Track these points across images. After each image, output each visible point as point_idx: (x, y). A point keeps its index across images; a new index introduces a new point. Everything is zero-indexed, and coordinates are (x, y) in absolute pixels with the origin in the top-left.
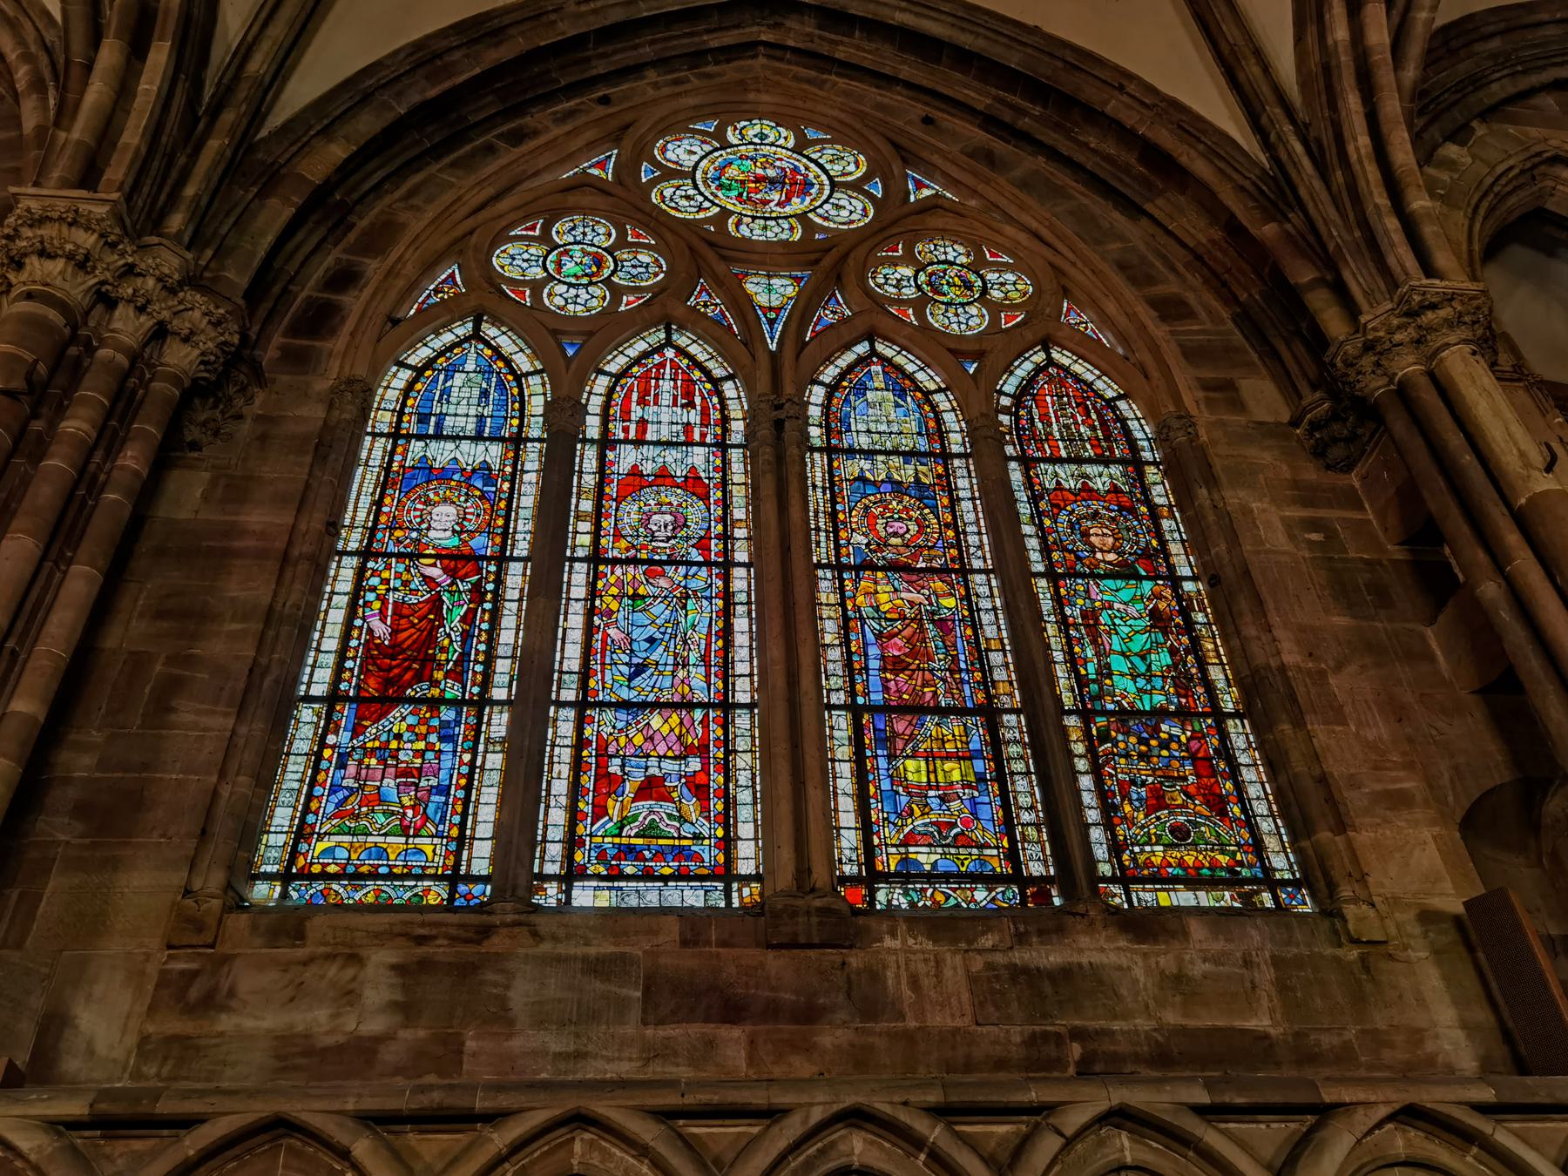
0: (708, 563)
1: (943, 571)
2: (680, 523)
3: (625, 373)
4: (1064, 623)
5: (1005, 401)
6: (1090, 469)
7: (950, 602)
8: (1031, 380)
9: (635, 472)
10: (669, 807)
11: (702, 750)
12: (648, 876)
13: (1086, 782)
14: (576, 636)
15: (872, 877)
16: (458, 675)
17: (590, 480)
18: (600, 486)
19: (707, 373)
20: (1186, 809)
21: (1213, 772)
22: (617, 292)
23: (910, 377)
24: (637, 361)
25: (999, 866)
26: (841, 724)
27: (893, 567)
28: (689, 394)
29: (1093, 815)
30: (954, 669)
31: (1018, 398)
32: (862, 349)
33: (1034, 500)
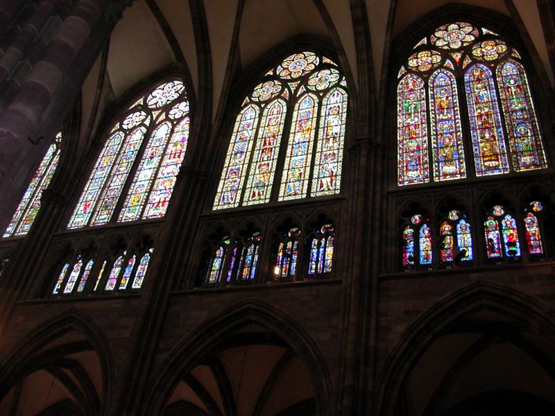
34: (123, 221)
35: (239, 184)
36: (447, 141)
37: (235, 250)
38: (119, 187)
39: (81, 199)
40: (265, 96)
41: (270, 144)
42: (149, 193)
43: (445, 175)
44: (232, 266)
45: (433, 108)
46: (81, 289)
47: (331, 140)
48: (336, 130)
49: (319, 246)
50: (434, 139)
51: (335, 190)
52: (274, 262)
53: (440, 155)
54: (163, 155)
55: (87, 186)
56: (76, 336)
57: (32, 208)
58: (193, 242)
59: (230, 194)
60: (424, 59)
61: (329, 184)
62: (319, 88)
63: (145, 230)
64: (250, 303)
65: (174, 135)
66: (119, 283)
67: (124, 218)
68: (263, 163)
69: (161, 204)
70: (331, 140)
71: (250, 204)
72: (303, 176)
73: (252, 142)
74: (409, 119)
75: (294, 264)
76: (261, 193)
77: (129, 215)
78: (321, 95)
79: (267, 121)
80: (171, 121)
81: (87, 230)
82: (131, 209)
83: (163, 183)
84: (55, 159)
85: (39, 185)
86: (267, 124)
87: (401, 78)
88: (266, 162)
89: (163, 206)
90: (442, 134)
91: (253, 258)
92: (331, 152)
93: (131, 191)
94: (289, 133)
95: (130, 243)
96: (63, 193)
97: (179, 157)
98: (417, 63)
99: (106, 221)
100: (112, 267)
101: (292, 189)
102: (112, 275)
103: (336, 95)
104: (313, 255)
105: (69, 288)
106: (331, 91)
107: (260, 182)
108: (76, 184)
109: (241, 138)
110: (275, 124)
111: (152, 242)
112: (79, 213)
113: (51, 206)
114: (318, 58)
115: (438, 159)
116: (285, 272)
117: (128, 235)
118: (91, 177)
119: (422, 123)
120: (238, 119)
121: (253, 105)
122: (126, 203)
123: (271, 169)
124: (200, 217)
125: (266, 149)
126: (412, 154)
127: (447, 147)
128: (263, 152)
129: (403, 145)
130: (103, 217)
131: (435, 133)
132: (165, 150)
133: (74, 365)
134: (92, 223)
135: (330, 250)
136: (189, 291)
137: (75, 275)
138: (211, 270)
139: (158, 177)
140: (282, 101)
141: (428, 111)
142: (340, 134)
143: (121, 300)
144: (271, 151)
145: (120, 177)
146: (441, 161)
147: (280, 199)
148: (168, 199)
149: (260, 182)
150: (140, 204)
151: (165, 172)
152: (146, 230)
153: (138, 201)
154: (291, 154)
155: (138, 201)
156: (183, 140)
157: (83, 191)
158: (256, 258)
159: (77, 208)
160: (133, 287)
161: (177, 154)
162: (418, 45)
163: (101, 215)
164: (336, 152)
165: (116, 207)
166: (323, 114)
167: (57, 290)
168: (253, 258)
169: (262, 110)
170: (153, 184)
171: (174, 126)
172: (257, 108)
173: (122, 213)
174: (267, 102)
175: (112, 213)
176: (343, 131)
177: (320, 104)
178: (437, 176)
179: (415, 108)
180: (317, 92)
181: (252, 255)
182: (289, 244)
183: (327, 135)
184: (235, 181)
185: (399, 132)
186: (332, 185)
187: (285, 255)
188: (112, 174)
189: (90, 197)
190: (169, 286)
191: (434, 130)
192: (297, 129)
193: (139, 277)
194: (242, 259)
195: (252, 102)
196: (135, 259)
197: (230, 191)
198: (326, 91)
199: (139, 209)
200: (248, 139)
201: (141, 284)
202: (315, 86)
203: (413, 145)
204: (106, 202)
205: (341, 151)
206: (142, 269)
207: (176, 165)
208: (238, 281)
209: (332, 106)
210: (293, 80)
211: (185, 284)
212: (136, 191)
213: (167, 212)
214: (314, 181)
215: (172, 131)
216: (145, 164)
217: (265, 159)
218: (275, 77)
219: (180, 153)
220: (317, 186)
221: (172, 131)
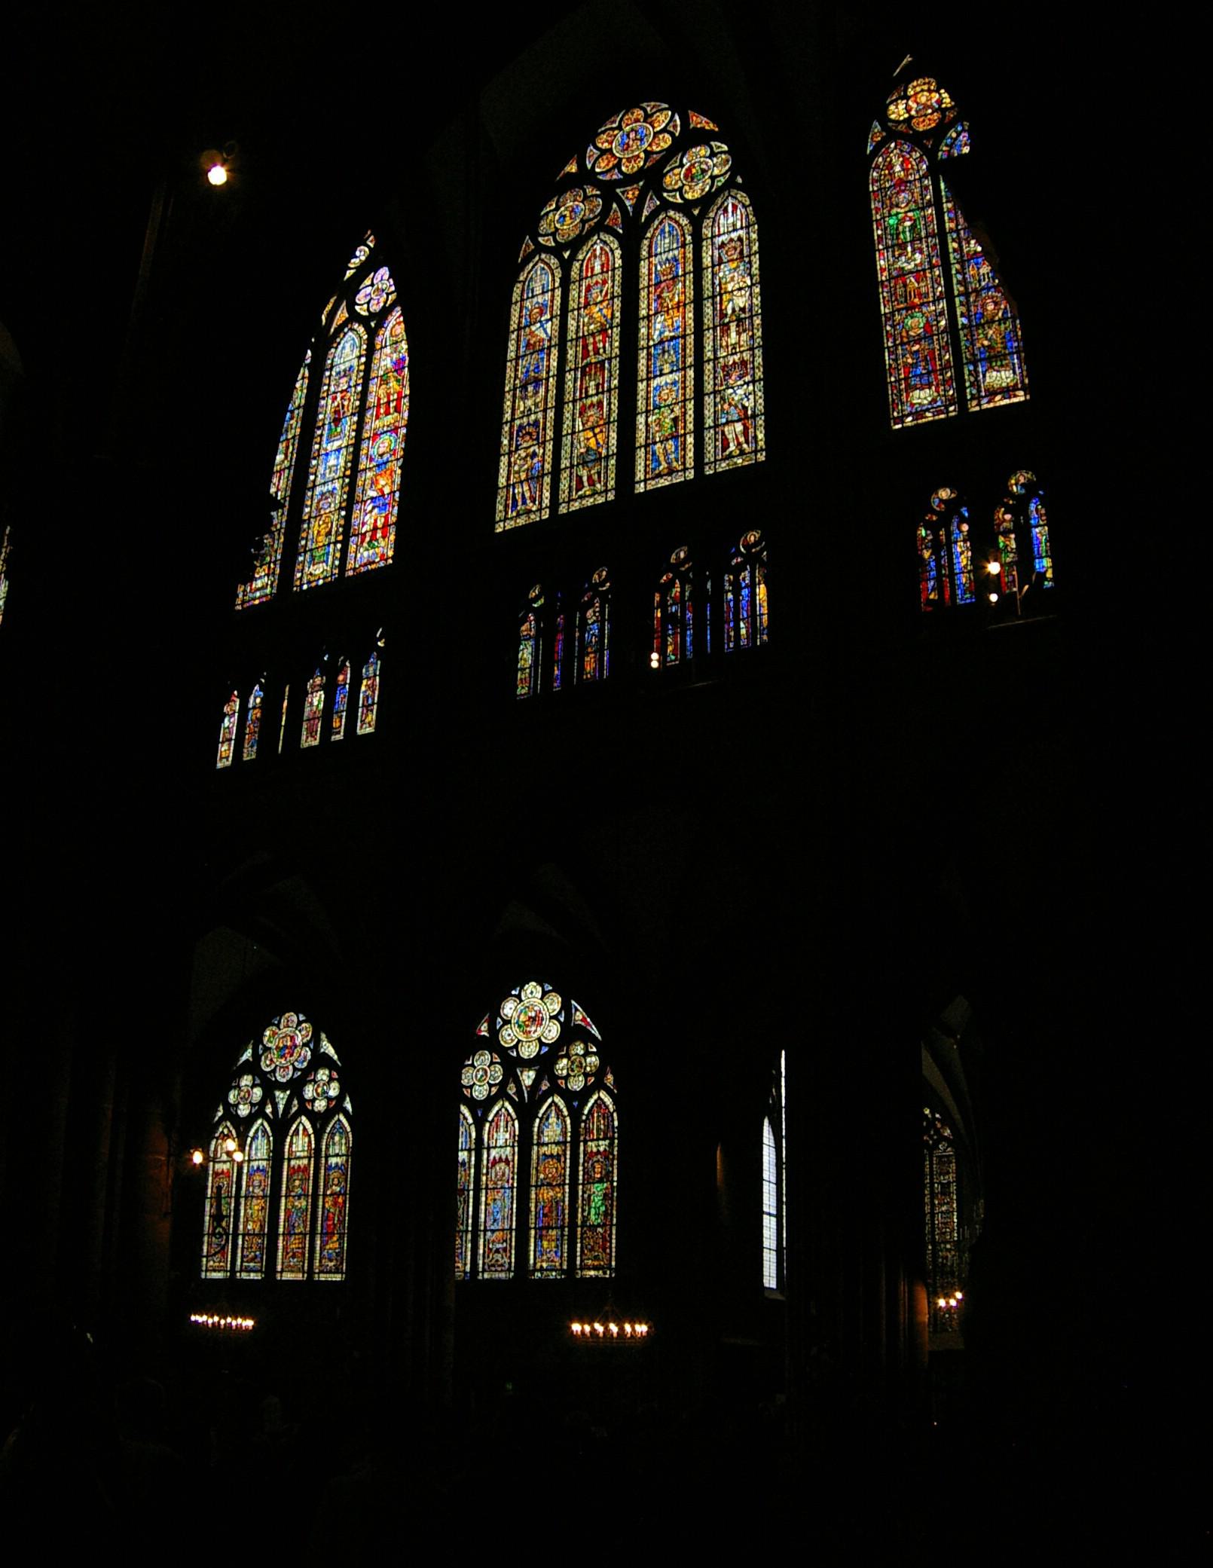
0: (509, 1188)
1: (558, 1185)
2: (504, 1174)
3: (493, 1120)
4: (583, 1200)
5: (584, 1118)
6: (601, 1143)
7: (559, 1195)
8: (592, 1107)
9: (495, 1158)
10: (500, 1255)
11: (506, 1241)
12: (496, 1271)
13: (579, 1245)
14: (483, 1211)
15: (535, 1270)
16: (462, 1224)
17: (485, 1162)
18: (488, 1162)
19: (511, 1117)
20: (599, 1253)
21: (606, 1240)
22: (491, 1086)
23: (561, 1111)
24: (496, 1115)
25: (559, 1268)
26: (533, 1232)
27: (549, 1184)
28: (507, 1127)
29: (578, 1254)
30: (557, 1215)
31: (587, 1116)
32: (550, 1100)
33: (585, 1155)
35: (544, 460)
36: (991, 307)
40: (569, 229)
41: (596, 352)
43: (992, 393)
45: (952, 225)
46: (249, 754)
47: (733, 326)
48: (741, 301)
49: (737, 589)
50: (961, 304)
51: (756, 452)
53: (978, 345)
54: (362, 411)
59: (526, 488)
60: (923, 99)
61: (742, 439)
62: (689, 196)
65: (377, 355)
66: (328, 730)
67: (305, 580)
68: (589, 401)
69: (379, 534)
70: (733, 326)
71: (576, 506)
72: (681, 424)
73: (555, 352)
74: (903, 258)
76: (596, 477)
77: (316, 571)
78: (699, 211)
79: (583, 294)
80: (364, 321)
82: (316, 554)
83: (374, 482)
86: (582, 300)
87: (875, 152)
88: (595, 399)
89: (384, 537)
90: (977, 292)
92: (736, 358)
93: (307, 510)
94: (636, 319)
97: (397, 409)
98: (908, 110)
99: (268, 590)
101: (662, 458)
103: (730, 209)
106: (720, 201)
107: (588, 449)
109: (528, 345)
110: (600, 299)
114: (677, 117)
115: (973, 354)
119: (932, 267)
120: (515, 297)
121: (543, 256)
123: (609, 416)
125: (589, 364)
126: (916, 348)
127: (991, 322)
128: (583, 374)
129: (893, 326)
130: (259, 584)
131: (962, 289)
132: (364, 395)
135: (762, 591)
139: (362, 467)
140: (609, 238)
141: (942, 234)
142: (751, 310)
144: (603, 368)
146: (981, 360)
147: (640, 488)
148: (393, 519)
149: (588, 449)
150: (333, 539)
151: (374, 452)
154: (648, 372)
155: (329, 534)
156: (398, 366)
160: (359, 732)
161: (392, 405)
162: (904, 62)
164: (746, 356)
166: (707, 261)
168: (601, 630)
169: (566, 266)
170: (352, 485)
171: (372, 334)
172: (554, 261)
174: (576, 244)
175: (278, 571)
176: (757, 301)
177: (698, 240)
178: (973, 398)
179: (913, 228)
180: (685, 208)
183: (723, 315)
184: (534, 455)
185: (884, 294)
186: (747, 442)
191: (959, 282)
192: (653, 306)
195: (541, 249)
197: (527, 480)
198: (707, 201)
200: (546, 344)
201: (373, 723)
202: (680, 190)
203: (916, 323)
205: (758, 352)
206: (369, 689)
207: (395, 430)
209: (724, 238)
210: (628, 180)
212: (318, 509)
214: (709, 435)
215: (371, 350)
216: (324, 438)
217: (592, 391)
218: (586, 177)
219: (399, 400)
220: (716, 447)
221: (371, 350)
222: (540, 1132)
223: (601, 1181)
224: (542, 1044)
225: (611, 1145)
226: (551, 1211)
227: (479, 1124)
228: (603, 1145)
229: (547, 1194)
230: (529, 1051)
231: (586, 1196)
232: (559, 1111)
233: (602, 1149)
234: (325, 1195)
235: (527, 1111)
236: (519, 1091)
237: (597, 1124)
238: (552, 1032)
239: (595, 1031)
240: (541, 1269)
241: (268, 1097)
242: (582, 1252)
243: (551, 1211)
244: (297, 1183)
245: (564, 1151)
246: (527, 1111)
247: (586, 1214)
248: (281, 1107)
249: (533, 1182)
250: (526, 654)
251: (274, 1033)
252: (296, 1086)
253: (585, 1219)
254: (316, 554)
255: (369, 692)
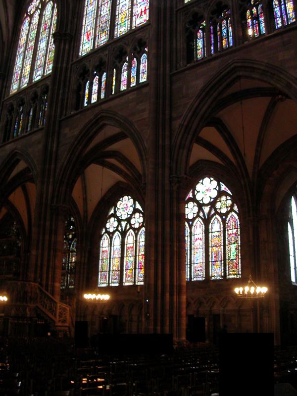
27: (216, 246)
34: (118, 36)
37: (212, 28)
38: (108, 12)
39: (83, 31)
42: (132, 8)
44: (213, 42)
46: (102, 96)
52: (245, 27)
55: (84, 21)
56: (111, 130)
57: (50, 52)
58: (176, 32)
63: (137, 36)
64: (236, 62)
67: (118, 34)
69: (143, 13)
75: (263, 25)
81: (94, 52)
82: (122, 25)
84: (54, 12)
85: (49, 34)
89: (145, 13)
91: (227, 31)
93: (117, 12)
95: (128, 49)
96: (69, 31)
100: (121, 73)
102: (123, 78)
104: (276, 14)
105: (94, 98)
108: (75, 22)
111: (145, 43)
112: (84, 42)
113: (63, 44)
116: (257, 33)
117: (125, 44)
118: (85, 14)
122: (117, 22)
124: (177, 11)
130: (102, 39)
133: (115, 154)
134: (96, 46)
136: (185, 68)
137: (95, 88)
138: (197, 50)
143: (135, 92)
145: (106, 5)
148: (147, 8)
150: (127, 19)
152: (139, 35)
153: (126, 17)
155: (126, 17)
157: (82, 26)
158: (230, 29)
159: (82, 39)
163: (101, 37)
165: (110, 28)
167: (87, 103)
168: (227, 31)
173: (116, 30)
181: (227, 29)
182: (254, 10)
187: (252, 19)
188: (100, 6)
189: (89, 28)
190: (168, 69)
193: (143, 73)
194: (219, 33)
196: (136, 61)
199: (128, 23)
201: (146, 78)
204: (102, 27)
206: (144, 66)
208: (223, 53)
211: (180, 65)
212: (121, 11)
213: (149, 18)
222: (212, 228)
223: (234, 243)
224: (211, 198)
225: (237, 231)
226: (217, 255)
227: (191, 226)
228: (235, 231)
229: (215, 249)
230: (206, 201)
231: (229, 249)
232: (218, 220)
233: (234, 233)
234: (139, 255)
235: (207, 221)
236: (204, 215)
237: (232, 224)
238: (214, 194)
239: (229, 192)
240: (214, 276)
241: (119, 224)
242: (229, 269)
243: (217, 255)
244: (130, 252)
245: (221, 234)
246: (207, 221)
247: (229, 255)
248: (124, 228)
249: (210, 246)
250: (200, 44)
251: (121, 204)
252: (128, 220)
253: (229, 257)
254: (122, 25)
255: (144, 68)
